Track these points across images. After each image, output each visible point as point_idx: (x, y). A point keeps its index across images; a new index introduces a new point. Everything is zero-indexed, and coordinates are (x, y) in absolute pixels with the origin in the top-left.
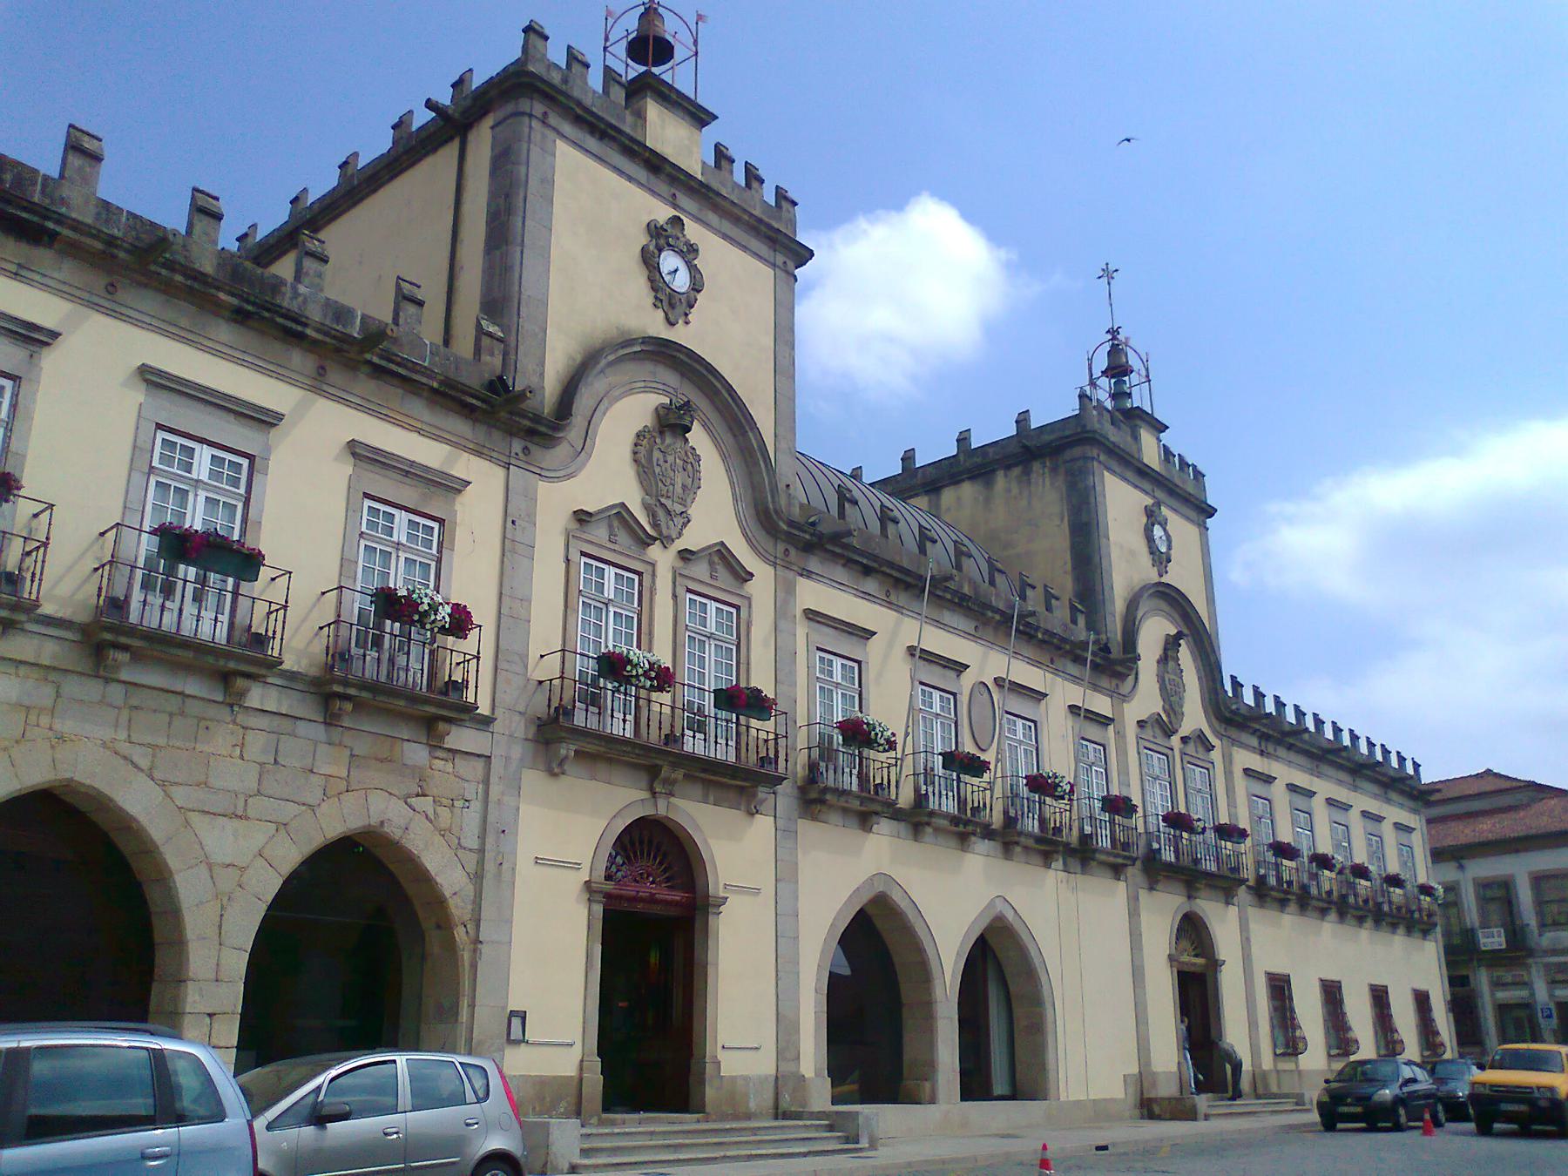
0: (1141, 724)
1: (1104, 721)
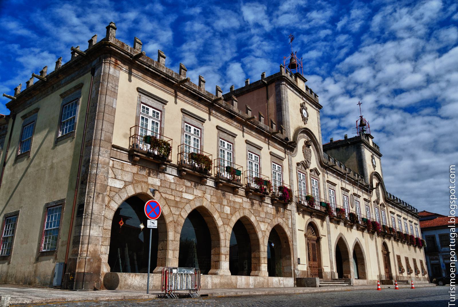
0: (374, 202)
1: (369, 201)
